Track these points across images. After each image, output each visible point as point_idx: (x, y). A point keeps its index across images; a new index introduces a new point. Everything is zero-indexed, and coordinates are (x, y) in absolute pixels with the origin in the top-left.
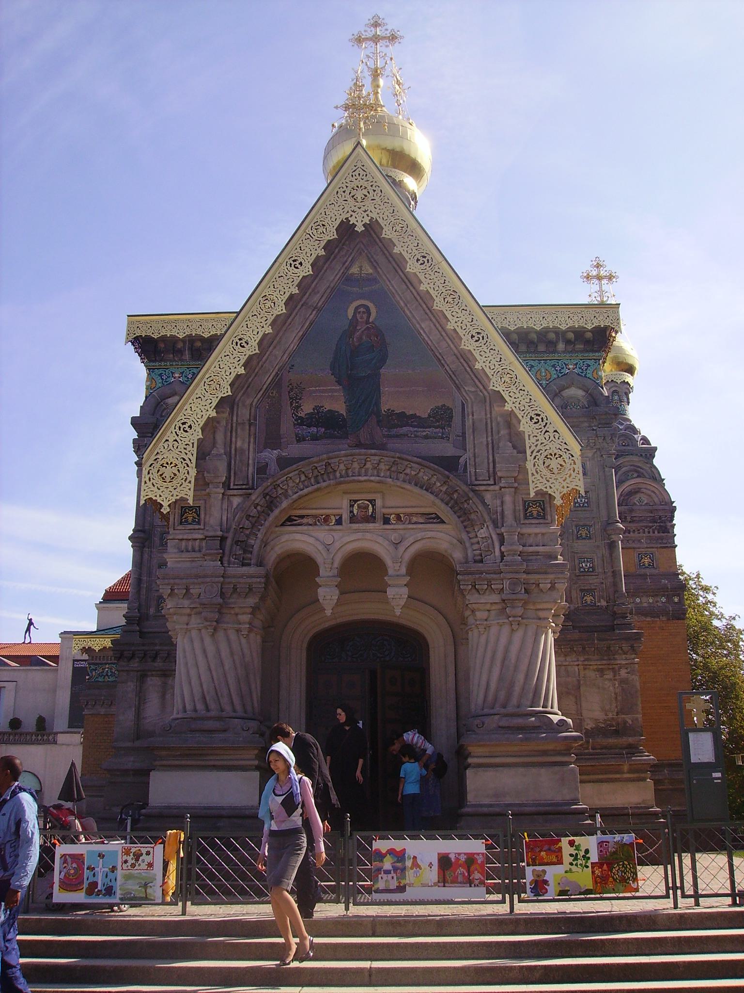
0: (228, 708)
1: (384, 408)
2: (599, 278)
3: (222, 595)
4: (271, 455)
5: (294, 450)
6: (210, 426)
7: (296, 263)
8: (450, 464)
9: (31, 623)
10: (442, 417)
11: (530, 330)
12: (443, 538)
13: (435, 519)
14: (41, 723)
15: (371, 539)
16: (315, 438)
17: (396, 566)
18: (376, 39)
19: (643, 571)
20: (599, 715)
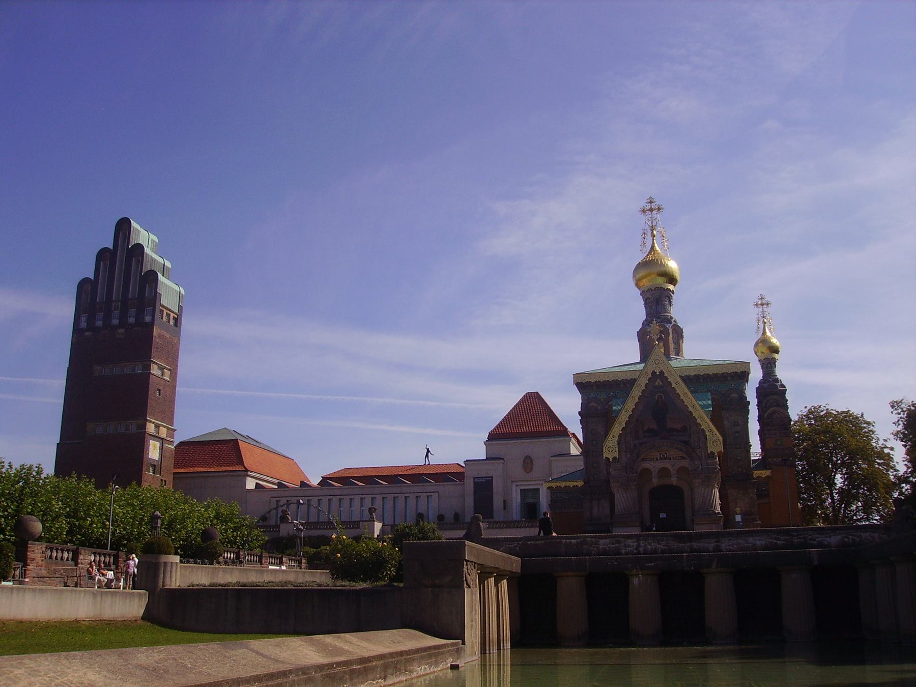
2: (762, 304)
6: (620, 435)
8: (686, 443)
9: (428, 451)
12: (685, 463)
13: (683, 458)
14: (456, 516)
15: (665, 464)
17: (673, 472)
18: (651, 210)
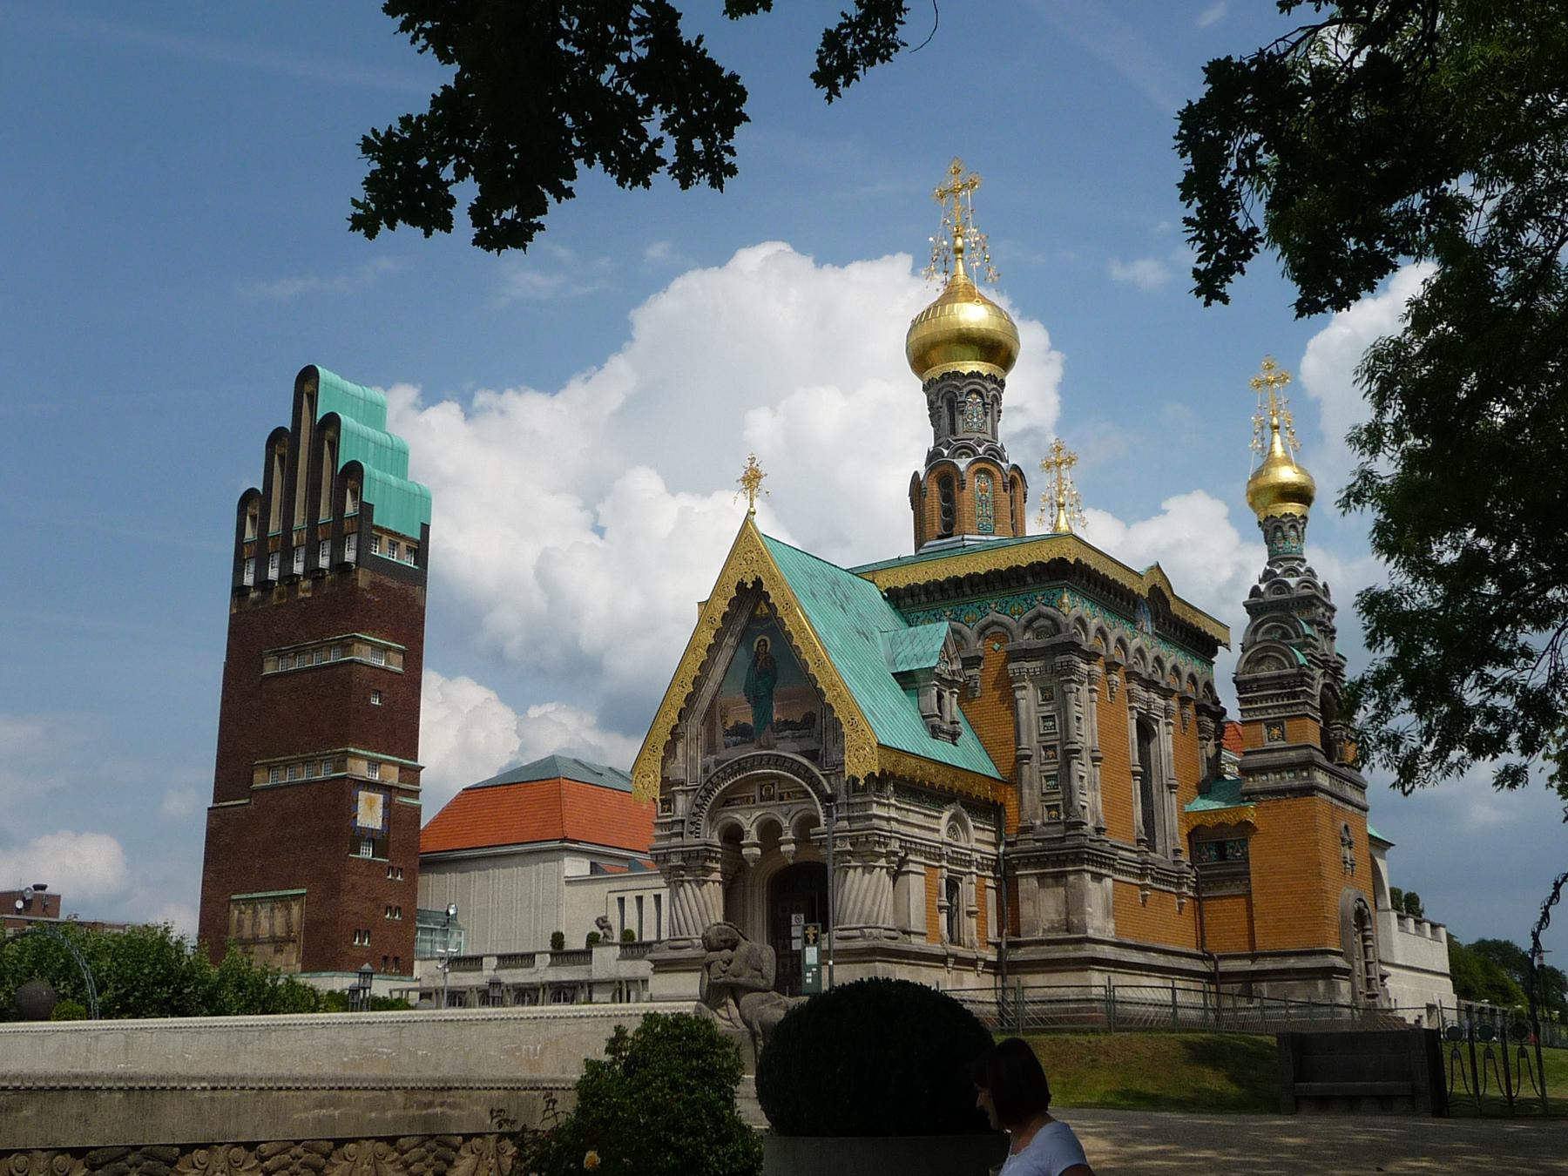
0: (693, 932)
1: (776, 717)
3: (683, 860)
4: (711, 759)
5: (723, 754)
7: (712, 620)
10: (809, 721)
11: (998, 572)
16: (736, 744)
19: (1269, 745)
20: (1054, 917)
